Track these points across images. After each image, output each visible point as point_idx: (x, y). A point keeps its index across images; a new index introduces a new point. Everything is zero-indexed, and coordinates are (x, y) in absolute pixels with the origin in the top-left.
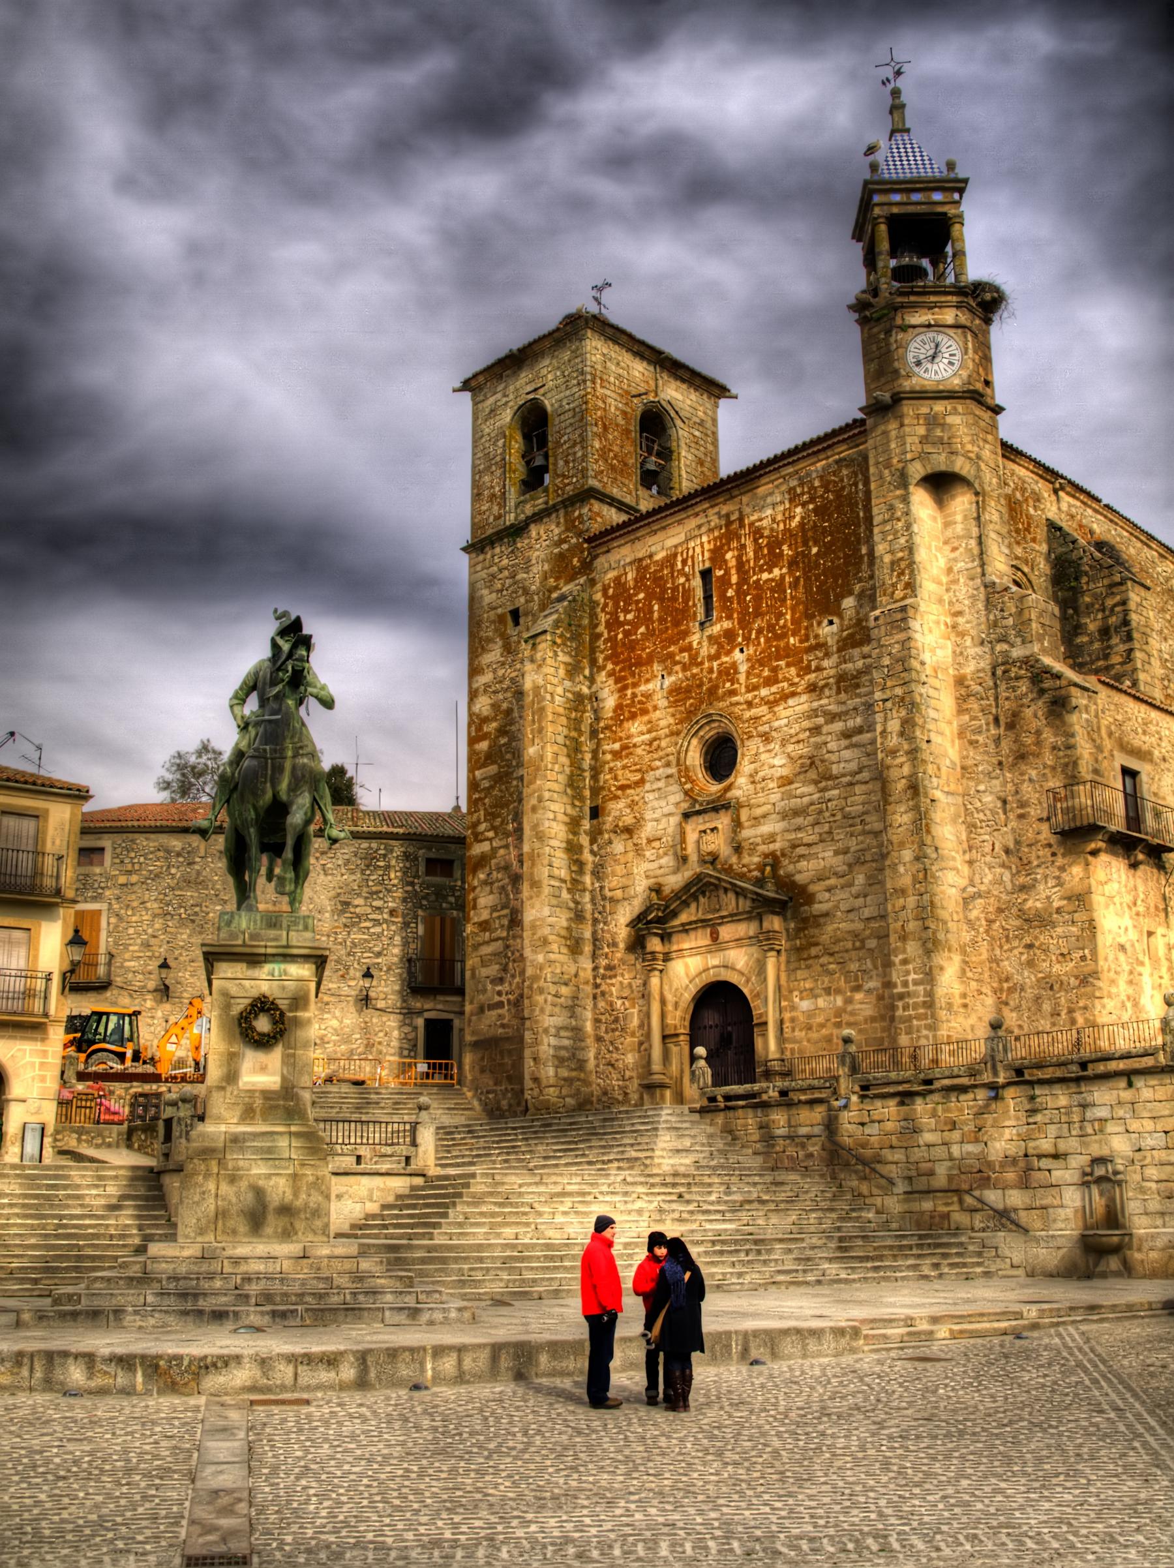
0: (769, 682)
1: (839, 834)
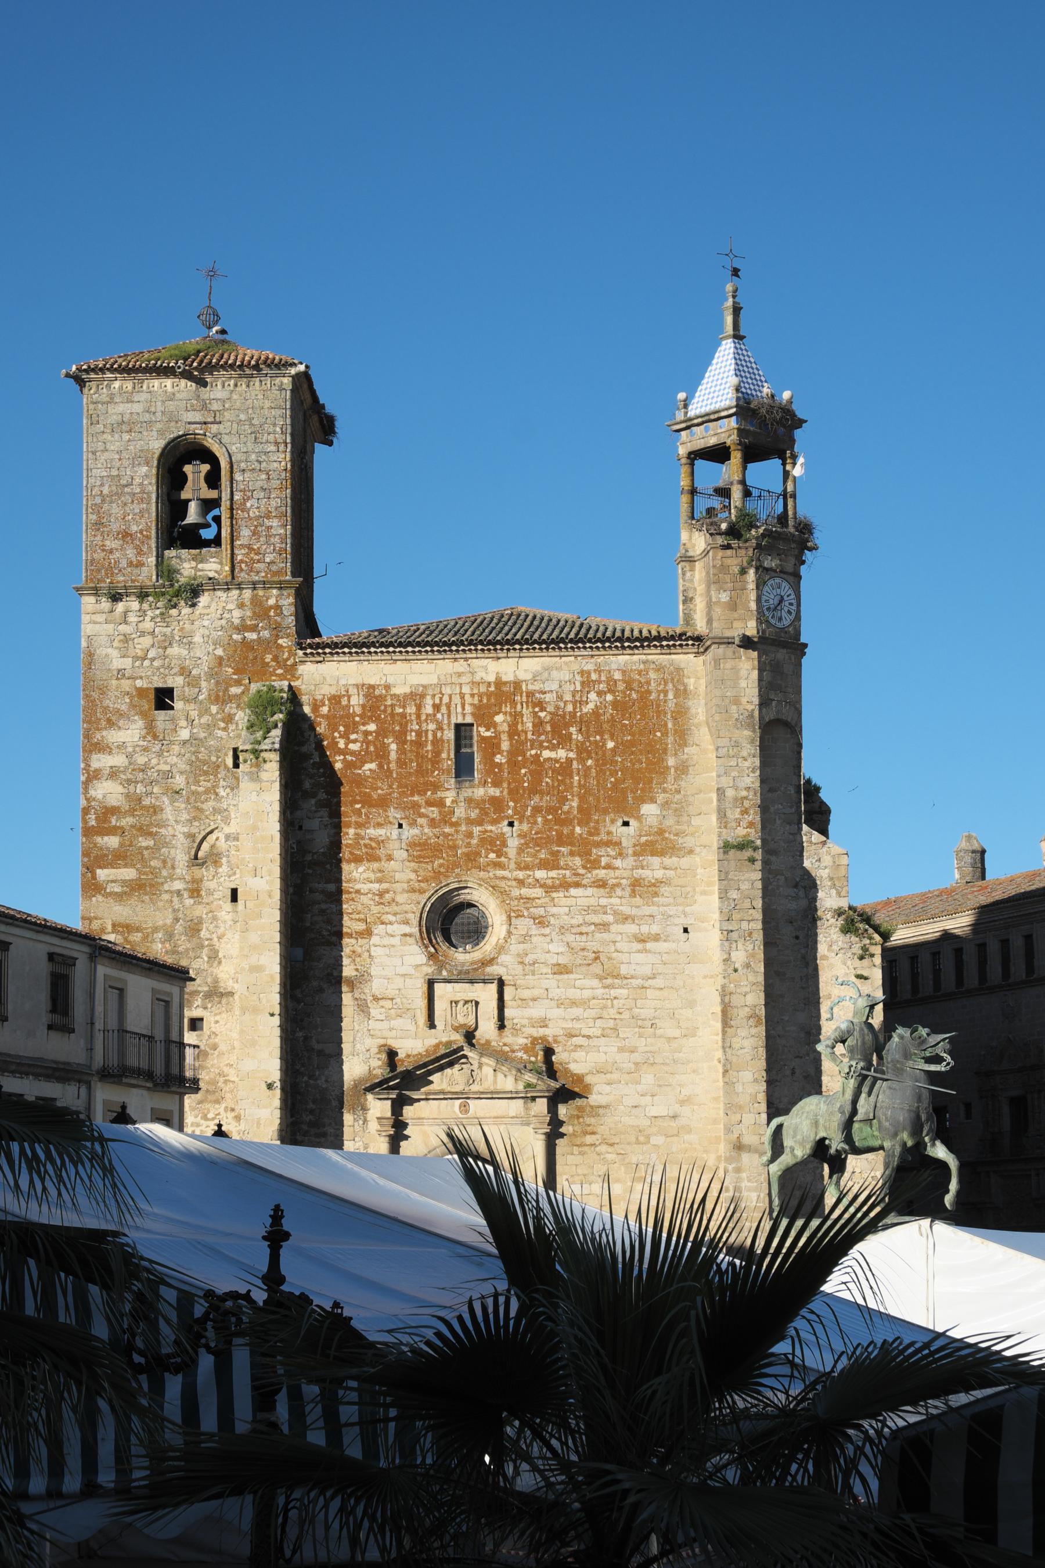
0: (544, 865)
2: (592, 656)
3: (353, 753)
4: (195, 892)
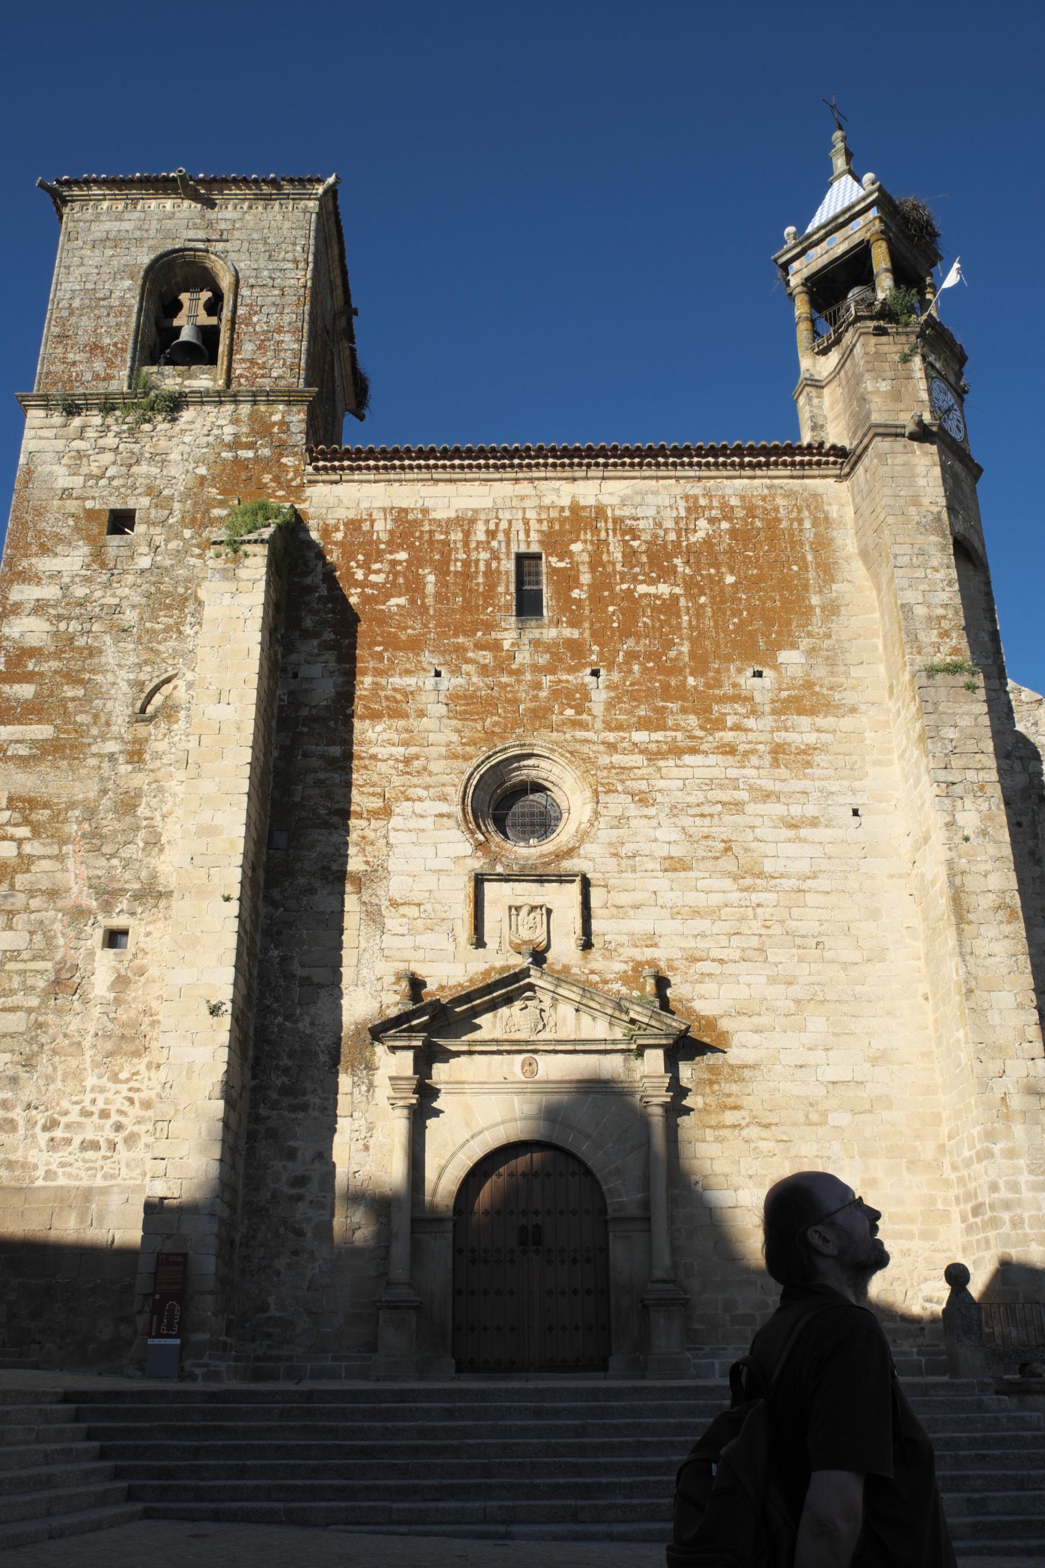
0: (644, 724)
2: (700, 478)
3: (374, 585)
4: (136, 755)
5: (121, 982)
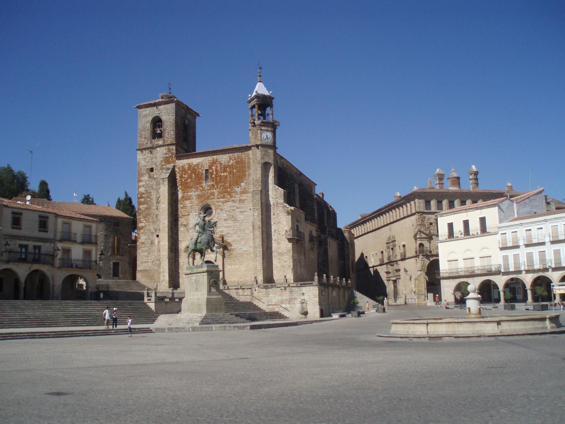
0: (223, 198)
1: (238, 232)
4: (157, 209)
5: (159, 242)
